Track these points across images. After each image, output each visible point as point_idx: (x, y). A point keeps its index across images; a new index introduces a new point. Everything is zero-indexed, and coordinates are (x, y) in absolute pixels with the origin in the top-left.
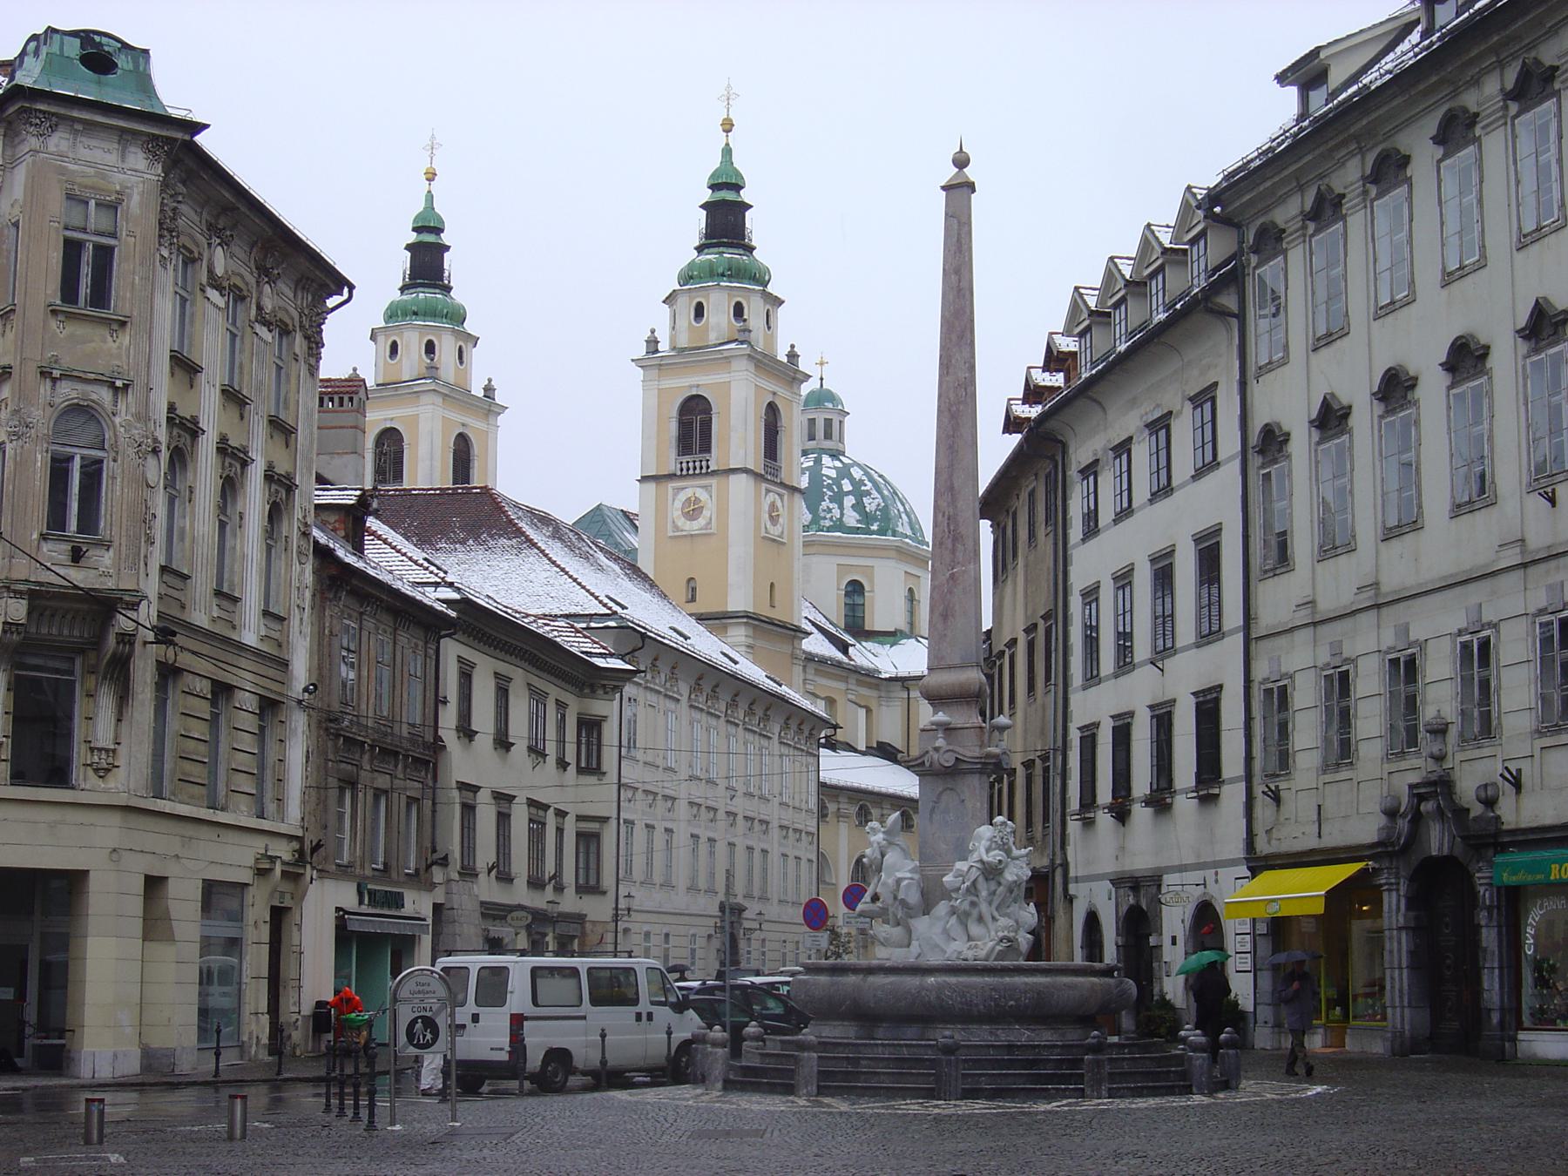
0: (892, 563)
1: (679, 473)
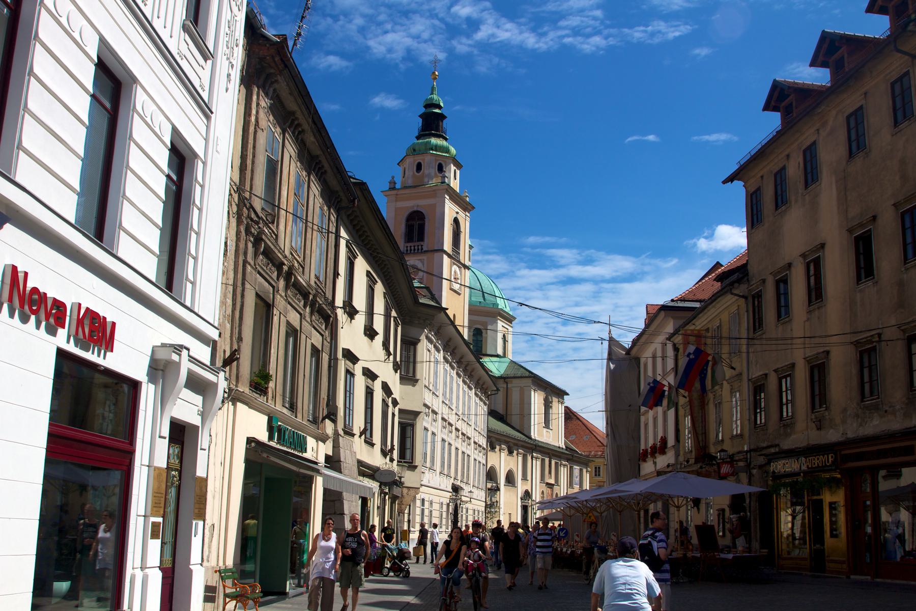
1: (405, 252)
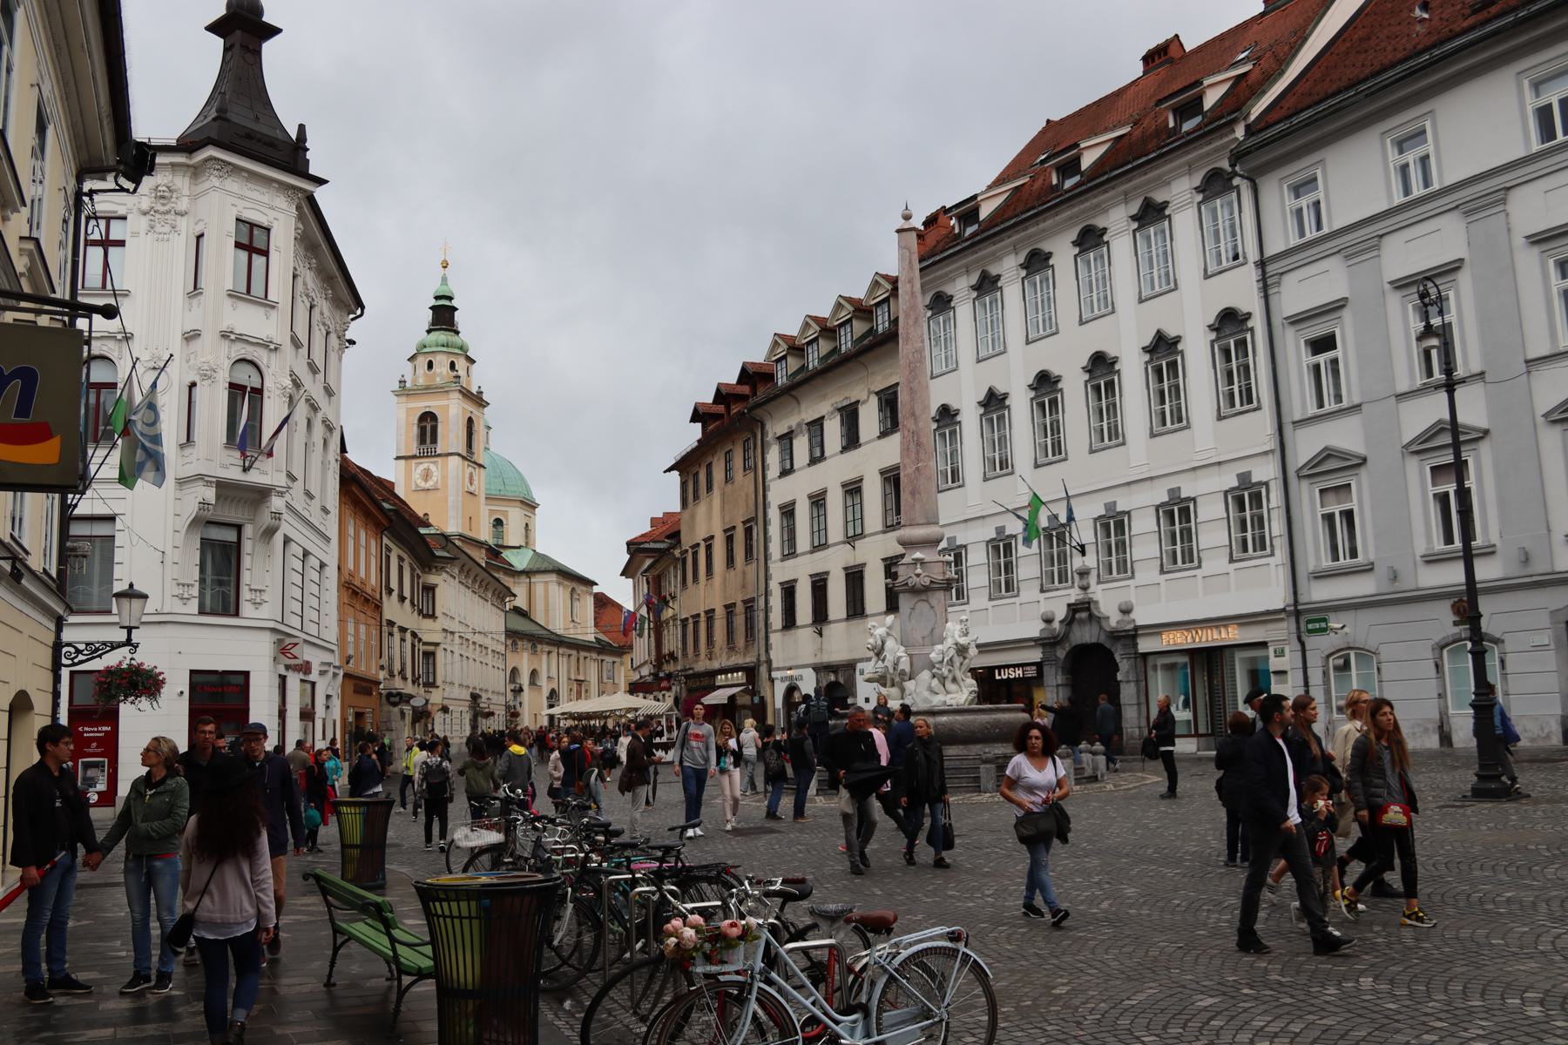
0: (518, 509)
